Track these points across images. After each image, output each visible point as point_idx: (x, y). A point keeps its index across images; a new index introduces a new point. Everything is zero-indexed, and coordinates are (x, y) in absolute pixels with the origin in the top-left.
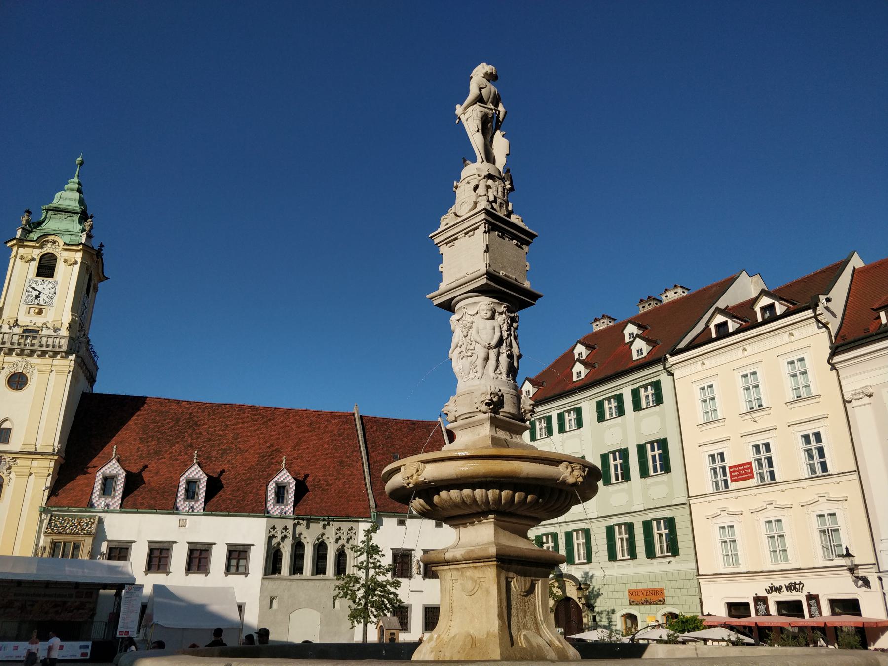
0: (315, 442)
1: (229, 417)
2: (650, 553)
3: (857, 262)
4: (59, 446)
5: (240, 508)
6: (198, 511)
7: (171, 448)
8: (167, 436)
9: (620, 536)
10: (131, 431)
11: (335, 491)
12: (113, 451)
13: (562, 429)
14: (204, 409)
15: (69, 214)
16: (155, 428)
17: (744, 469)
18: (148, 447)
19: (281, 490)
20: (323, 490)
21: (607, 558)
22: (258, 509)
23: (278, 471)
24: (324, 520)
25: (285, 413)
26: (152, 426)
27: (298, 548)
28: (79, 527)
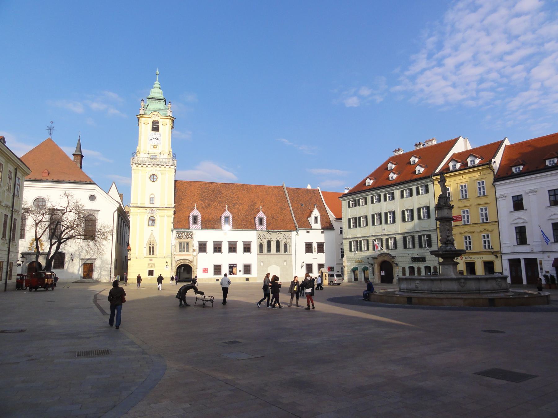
0: (269, 199)
1: (233, 189)
2: (421, 246)
3: (507, 143)
4: (175, 204)
5: (246, 228)
7: (214, 203)
9: (409, 240)
10: (197, 197)
11: (281, 219)
13: (385, 200)
14: (223, 186)
17: (458, 217)
18: (205, 203)
19: (261, 220)
20: (276, 220)
21: (403, 248)
22: (253, 227)
23: (259, 211)
24: (278, 231)
25: (255, 187)
26: (204, 194)
27: (269, 242)
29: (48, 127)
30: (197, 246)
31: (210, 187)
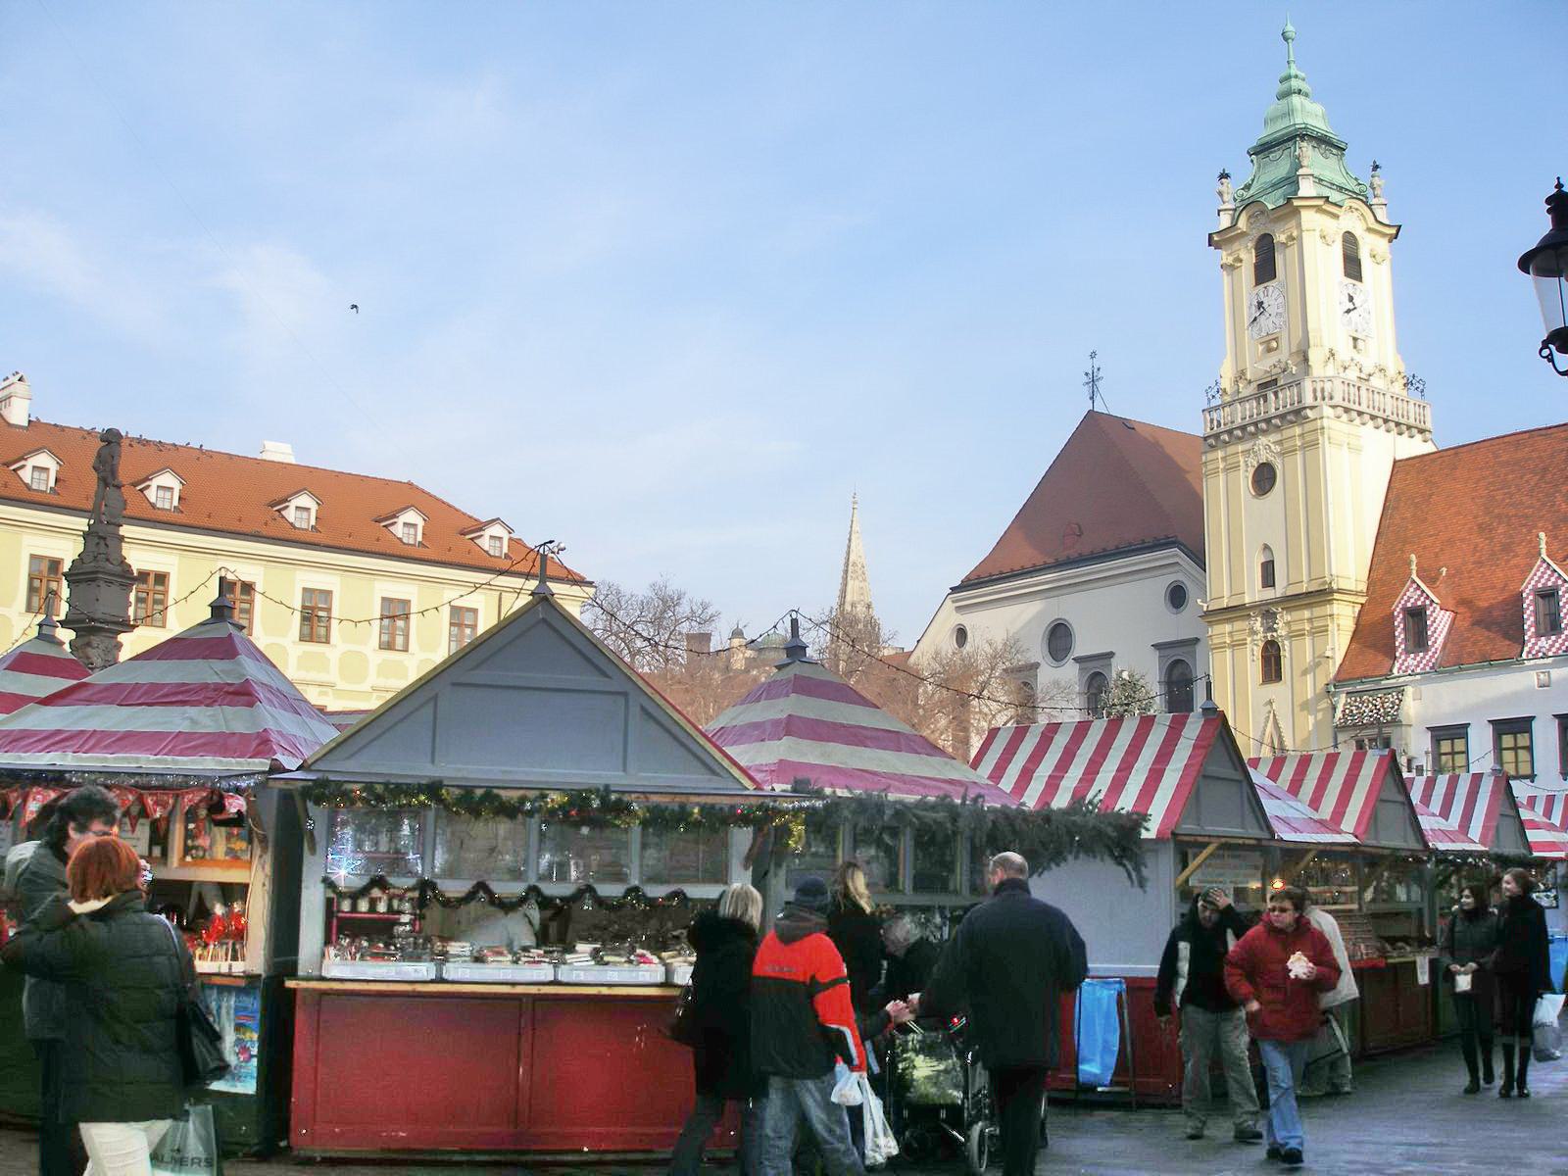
6: (1413, 671)
8: (1527, 508)
12: (1547, 543)
15: (1283, 146)
16: (1503, 500)
28: (1382, 710)
29: (1087, 374)
30: (1427, 753)
31: (1534, 455)
